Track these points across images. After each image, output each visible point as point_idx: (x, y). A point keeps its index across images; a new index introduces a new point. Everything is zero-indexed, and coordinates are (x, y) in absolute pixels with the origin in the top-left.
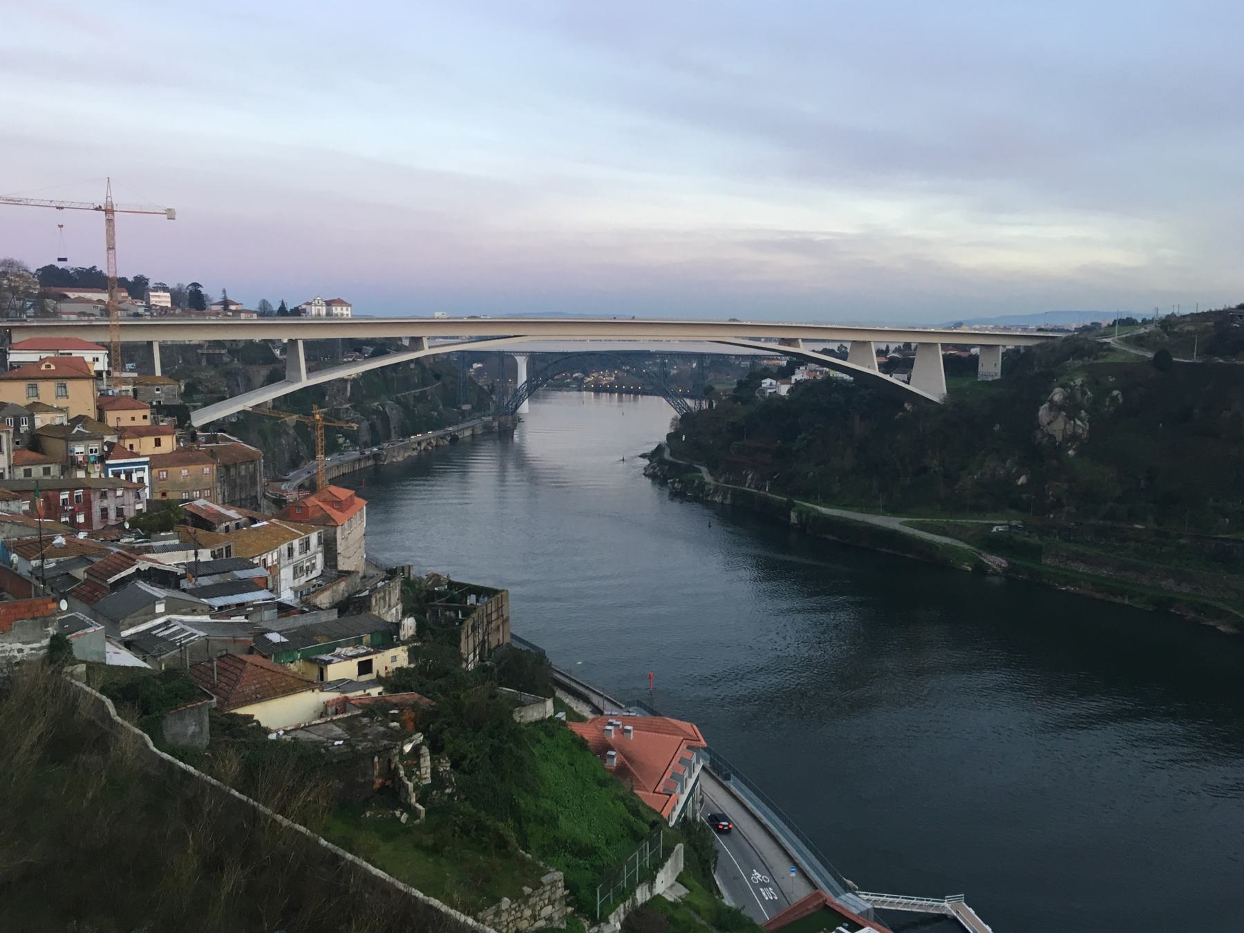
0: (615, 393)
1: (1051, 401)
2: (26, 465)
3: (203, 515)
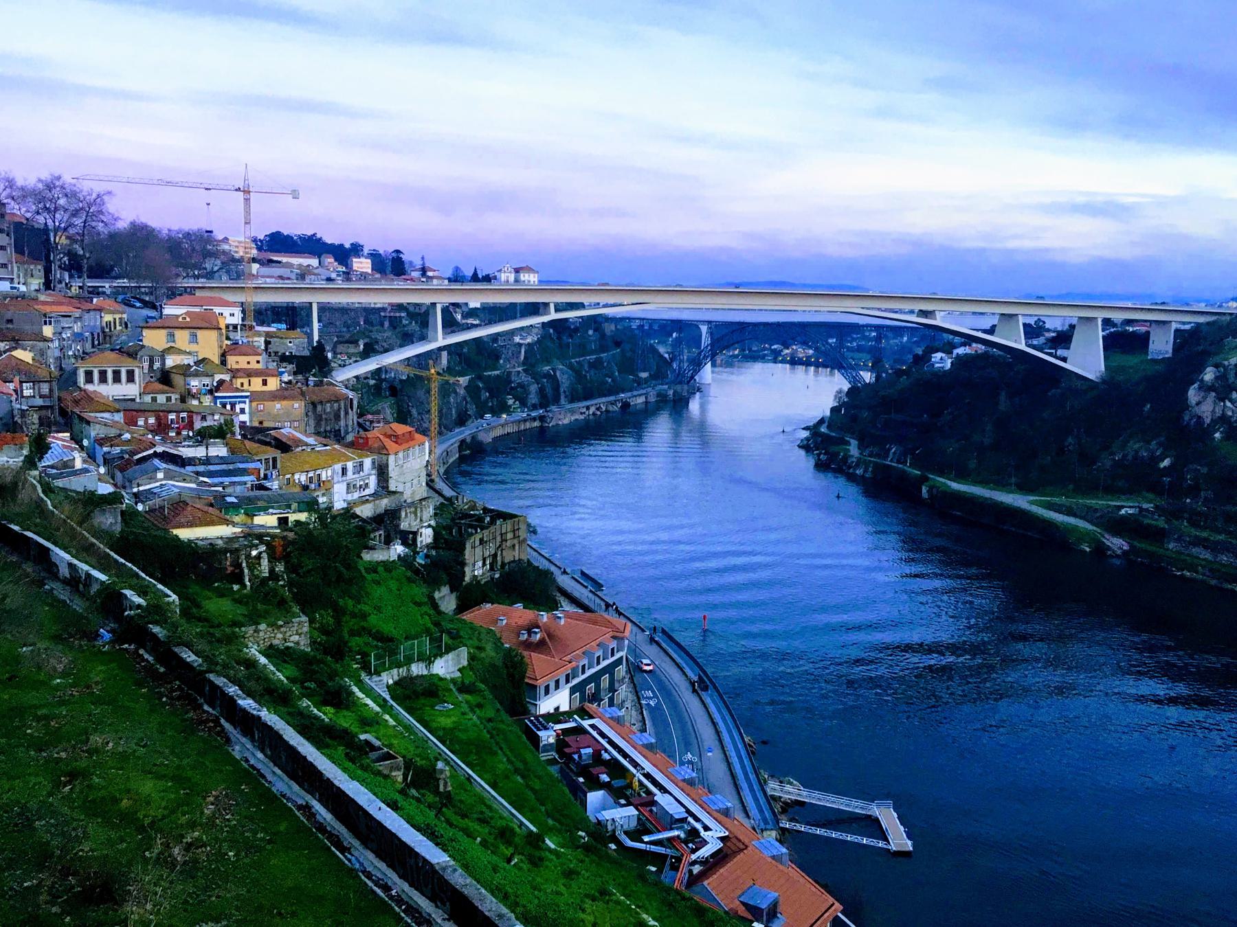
0: (811, 366)
3: (284, 440)
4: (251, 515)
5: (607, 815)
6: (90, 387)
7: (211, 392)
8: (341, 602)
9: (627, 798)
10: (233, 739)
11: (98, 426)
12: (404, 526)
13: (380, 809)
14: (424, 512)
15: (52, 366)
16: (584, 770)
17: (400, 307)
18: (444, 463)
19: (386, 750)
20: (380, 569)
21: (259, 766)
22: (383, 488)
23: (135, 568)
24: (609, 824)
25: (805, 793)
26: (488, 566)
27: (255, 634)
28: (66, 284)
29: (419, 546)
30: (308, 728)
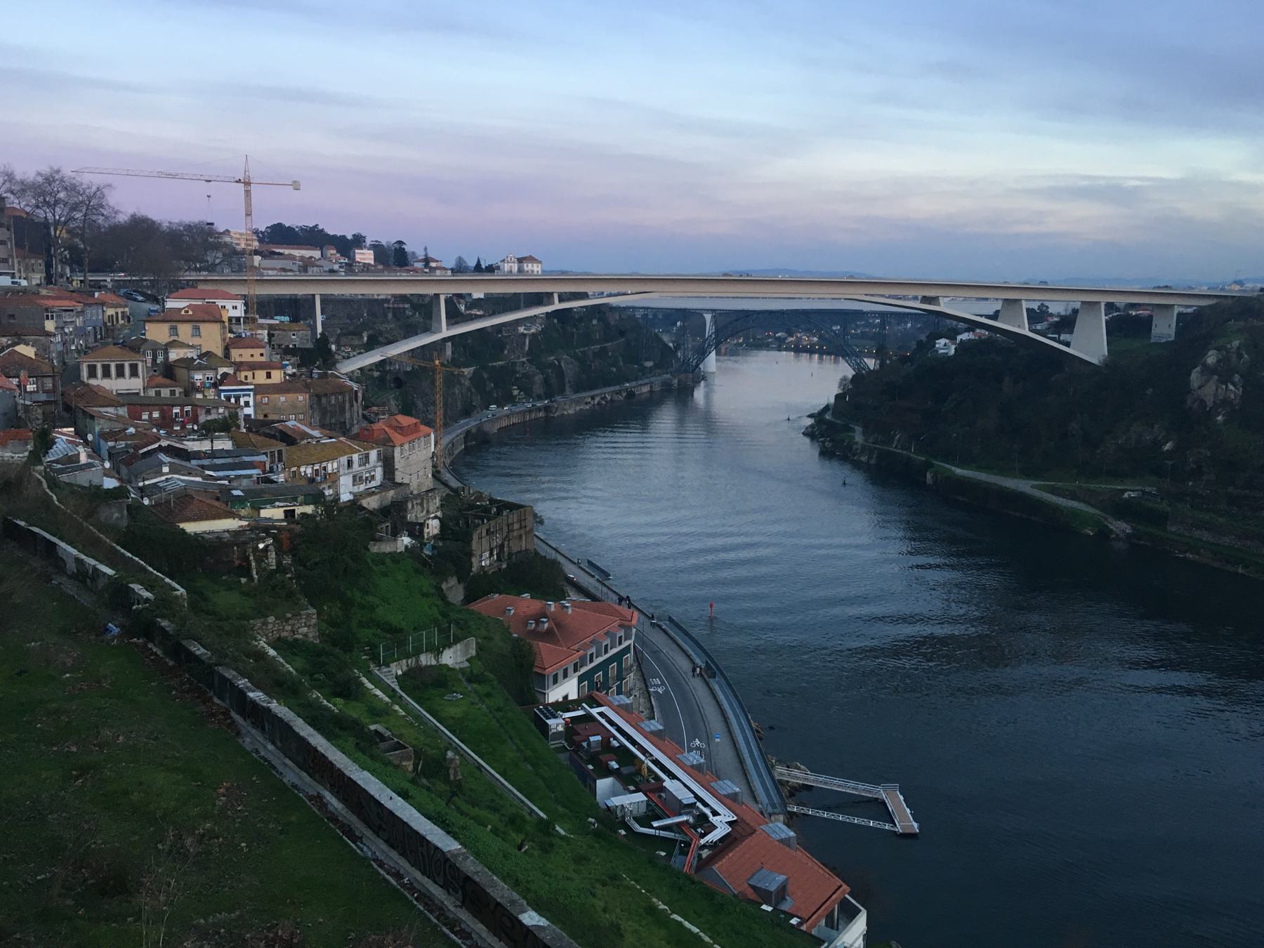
1: (1205, 365)
2: (158, 387)
3: (289, 433)
4: (258, 509)
5: (616, 801)
6: (93, 382)
7: (215, 385)
8: (349, 594)
9: (635, 784)
10: (243, 731)
11: (102, 421)
12: (410, 517)
13: (391, 798)
14: (430, 504)
15: (55, 361)
16: (593, 758)
17: (403, 298)
18: (450, 454)
19: (396, 740)
20: (388, 561)
21: (270, 757)
22: (389, 479)
23: (142, 562)
24: (618, 812)
25: (813, 778)
26: (495, 557)
27: (264, 627)
28: (68, 278)
29: (426, 537)
30: (318, 720)
